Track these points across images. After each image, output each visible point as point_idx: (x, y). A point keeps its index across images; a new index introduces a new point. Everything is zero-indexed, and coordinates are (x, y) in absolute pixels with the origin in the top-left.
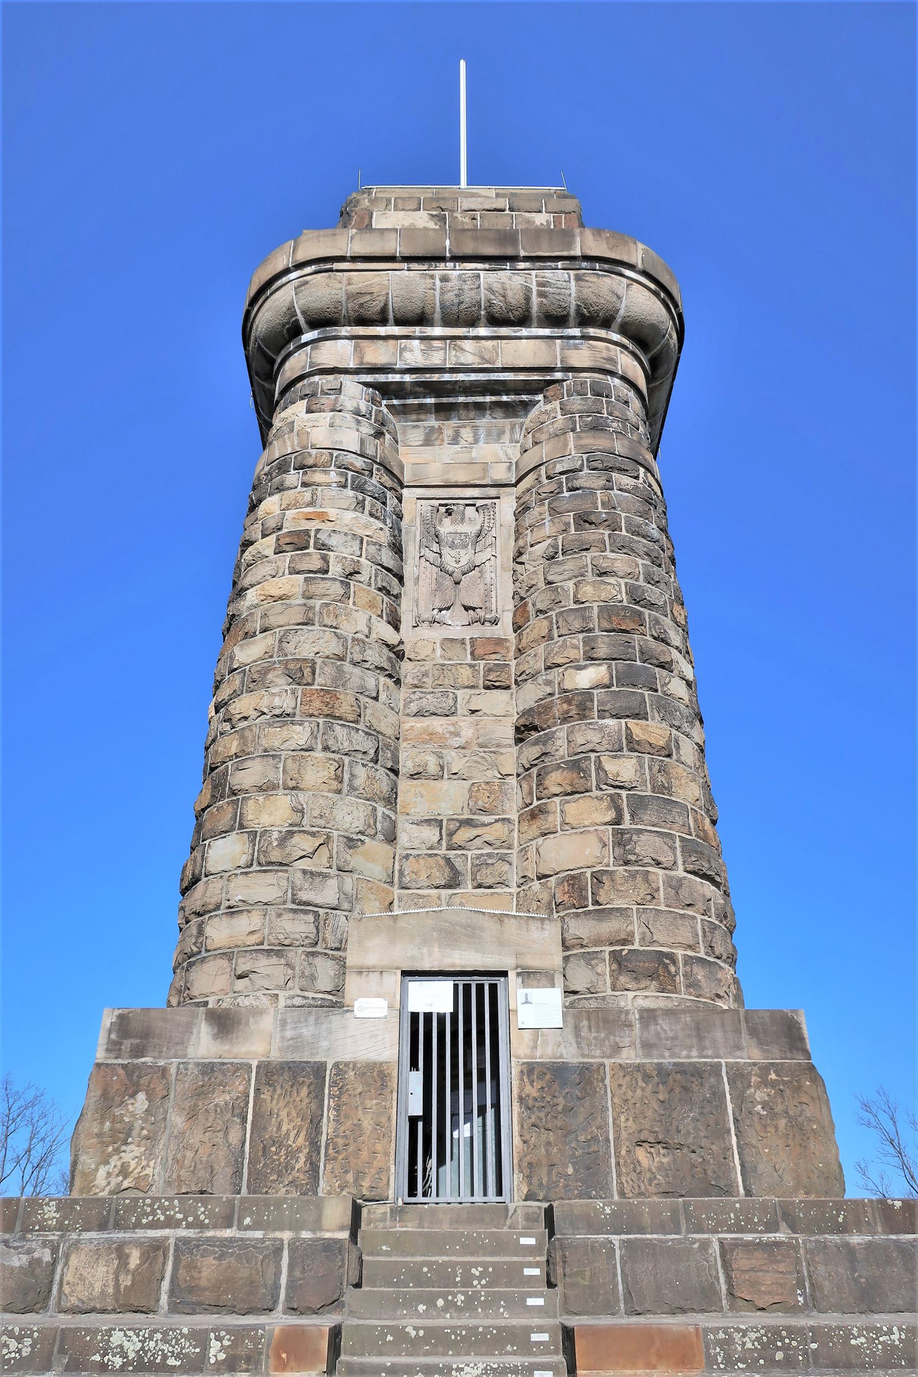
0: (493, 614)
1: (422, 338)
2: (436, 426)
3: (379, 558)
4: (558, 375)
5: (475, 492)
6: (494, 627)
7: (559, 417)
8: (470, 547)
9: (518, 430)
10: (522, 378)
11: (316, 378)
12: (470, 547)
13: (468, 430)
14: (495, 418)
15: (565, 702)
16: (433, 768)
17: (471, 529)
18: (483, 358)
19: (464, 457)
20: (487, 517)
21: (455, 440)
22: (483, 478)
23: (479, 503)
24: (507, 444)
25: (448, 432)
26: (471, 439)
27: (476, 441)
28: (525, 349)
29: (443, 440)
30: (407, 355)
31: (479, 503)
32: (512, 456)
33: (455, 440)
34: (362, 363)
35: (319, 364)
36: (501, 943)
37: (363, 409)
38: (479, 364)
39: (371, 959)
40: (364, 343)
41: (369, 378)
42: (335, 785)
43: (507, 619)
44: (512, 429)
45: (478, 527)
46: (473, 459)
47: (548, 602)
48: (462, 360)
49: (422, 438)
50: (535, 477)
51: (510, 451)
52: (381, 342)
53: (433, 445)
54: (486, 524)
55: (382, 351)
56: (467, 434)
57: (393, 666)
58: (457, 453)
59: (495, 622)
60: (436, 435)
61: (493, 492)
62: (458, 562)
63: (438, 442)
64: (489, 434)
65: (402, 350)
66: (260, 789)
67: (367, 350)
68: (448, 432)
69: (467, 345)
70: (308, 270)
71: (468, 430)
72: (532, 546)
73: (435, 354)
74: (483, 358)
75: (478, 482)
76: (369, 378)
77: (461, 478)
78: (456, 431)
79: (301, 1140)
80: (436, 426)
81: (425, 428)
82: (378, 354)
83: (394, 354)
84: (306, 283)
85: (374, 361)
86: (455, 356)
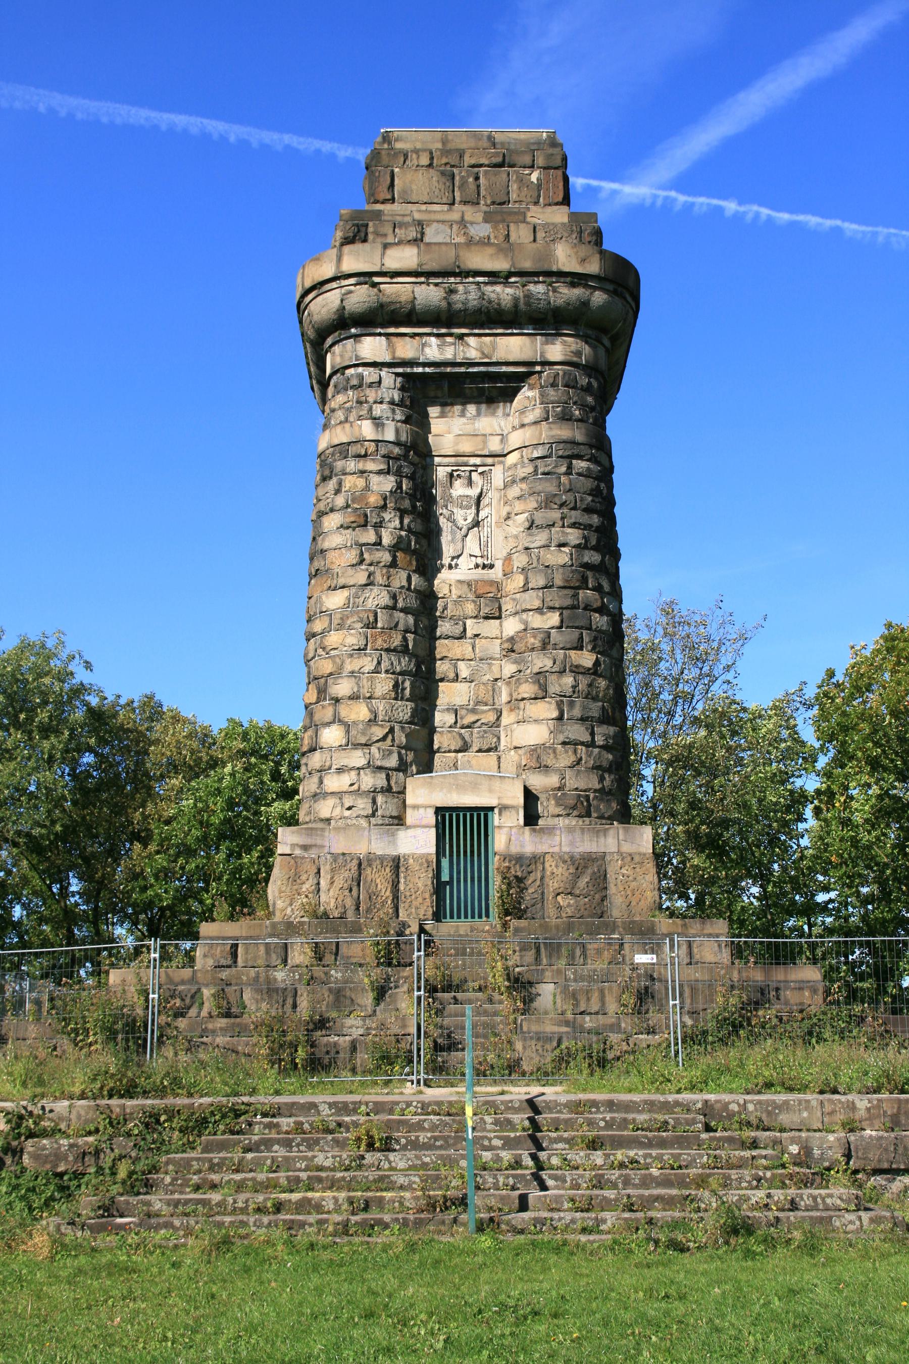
1: (438, 336)
4: (538, 368)
5: (478, 461)
6: (491, 571)
11: (360, 369)
16: (452, 675)
18: (483, 353)
19: (469, 429)
21: (463, 414)
22: (483, 449)
23: (480, 469)
28: (513, 347)
30: (427, 350)
31: (480, 469)
33: (463, 414)
34: (394, 358)
36: (490, 791)
37: (396, 398)
39: (420, 801)
40: (394, 339)
41: (400, 370)
43: (499, 565)
45: (479, 491)
48: (468, 355)
51: (502, 424)
52: (407, 338)
55: (409, 346)
61: (489, 461)
65: (424, 345)
66: (350, 698)
69: (472, 341)
70: (352, 281)
73: (447, 349)
74: (483, 353)
75: (480, 453)
76: (400, 370)
77: (466, 447)
79: (388, 893)
82: (406, 349)
83: (417, 349)
84: (351, 292)
85: (403, 356)
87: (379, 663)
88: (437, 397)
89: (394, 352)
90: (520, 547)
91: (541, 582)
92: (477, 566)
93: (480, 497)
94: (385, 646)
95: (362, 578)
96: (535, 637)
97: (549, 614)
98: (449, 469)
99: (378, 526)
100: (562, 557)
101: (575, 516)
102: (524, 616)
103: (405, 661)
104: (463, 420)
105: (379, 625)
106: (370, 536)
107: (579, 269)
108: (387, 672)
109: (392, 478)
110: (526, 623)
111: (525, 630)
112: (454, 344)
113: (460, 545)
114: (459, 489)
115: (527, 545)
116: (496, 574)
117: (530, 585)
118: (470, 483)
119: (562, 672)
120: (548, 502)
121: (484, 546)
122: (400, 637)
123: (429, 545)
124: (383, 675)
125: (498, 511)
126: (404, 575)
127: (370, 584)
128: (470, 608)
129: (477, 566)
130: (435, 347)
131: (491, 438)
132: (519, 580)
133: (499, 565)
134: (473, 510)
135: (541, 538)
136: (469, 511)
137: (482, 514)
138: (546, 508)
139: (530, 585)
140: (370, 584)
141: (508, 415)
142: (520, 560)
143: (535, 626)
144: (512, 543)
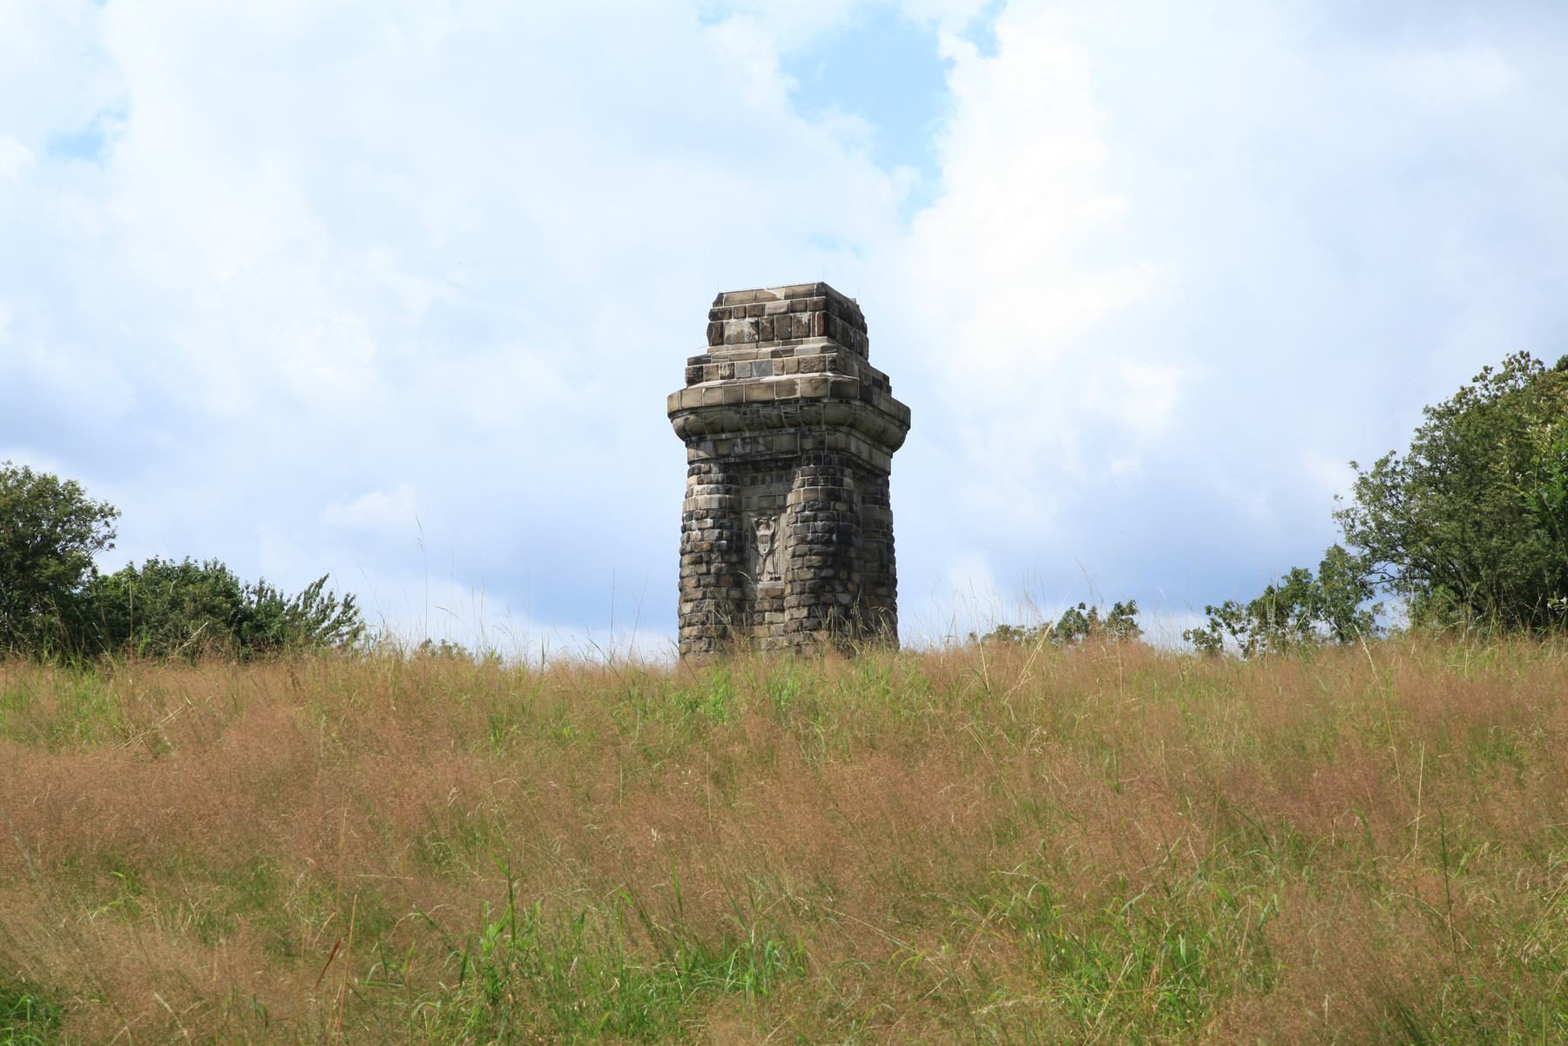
56: (768, 479)
93: (773, 535)
95: (699, 595)
99: (709, 563)
100: (809, 574)
101: (816, 547)
106: (703, 568)
107: (813, 395)
109: (717, 531)
116: (780, 584)
120: (803, 541)
121: (775, 566)
126: (724, 590)
127: (704, 597)
128: (767, 606)
135: (799, 562)
140: (704, 597)
142: (790, 577)
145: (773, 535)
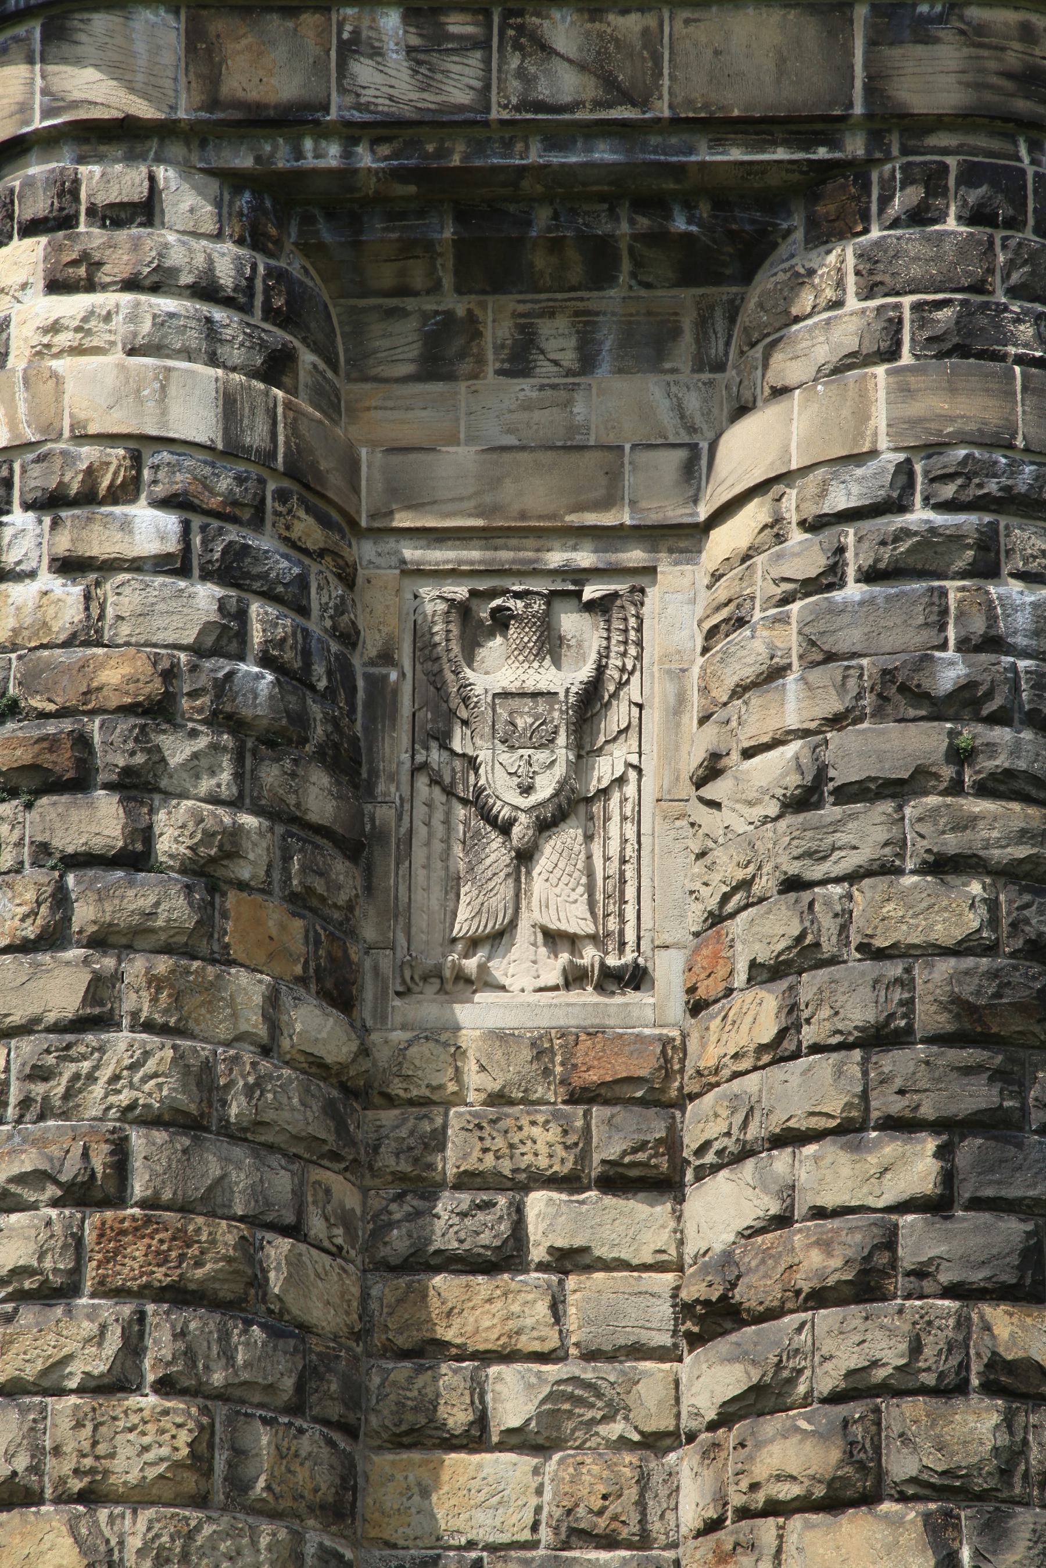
0: (629, 957)
2: (461, 311)
3: (292, 800)
6: (632, 997)
7: (852, 303)
8: (562, 740)
9: (720, 325)
10: (736, 154)
12: (562, 740)
13: (562, 323)
14: (648, 286)
15: (818, 1243)
17: (567, 678)
19: (547, 422)
20: (616, 637)
24: (686, 373)
25: (498, 329)
26: (569, 358)
27: (587, 362)
29: (481, 361)
32: (699, 421)
33: (520, 361)
34: (213, 103)
35: (75, 105)
37: (226, 274)
38: (598, 104)
42: (190, 1482)
43: (669, 972)
44: (703, 324)
45: (585, 672)
46: (573, 429)
47: (780, 946)
48: (543, 91)
49: (414, 351)
50: (765, 518)
51: (693, 402)
53: (450, 377)
54: (615, 661)
55: (279, 53)
56: (558, 341)
57: (341, 1128)
58: (527, 406)
59: (636, 978)
60: (459, 342)
61: (635, 556)
62: (527, 790)
63: (465, 367)
64: (628, 339)
67: (230, 47)
68: (498, 329)
71: (562, 323)
72: (748, 753)
73: (453, 65)
74: (609, 82)
78: (522, 328)
80: (461, 311)
81: (425, 316)
83: (319, 66)
85: (253, 95)
86: (521, 74)
87: (133, 1347)
88: (403, 291)
89: (212, 79)
90: (766, 884)
91: (859, 1012)
92: (574, 978)
93: (591, 701)
94: (160, 1275)
96: (825, 1245)
97: (891, 1148)
98: (460, 591)
102: (781, 1160)
103: (249, 1342)
104: (524, 388)
105: (138, 1188)
108: (165, 1386)
110: (789, 1191)
111: (782, 1221)
112: (483, 44)
113: (506, 890)
114: (498, 669)
115: (793, 868)
117: (809, 1035)
118: (550, 645)
119: (951, 1389)
121: (606, 895)
122: (227, 1236)
123: (369, 889)
124: (151, 1401)
125: (670, 751)
126: (249, 988)
127: (95, 1018)
129: (574, 978)
130: (396, 58)
131: (644, 457)
132: (759, 1015)
133: (669, 972)
134: (562, 752)
136: (542, 756)
137: (605, 769)
138: (879, 714)
139: (809, 1035)
140: (95, 1018)
141: (719, 367)
142: (764, 931)
143: (829, 1200)
144: (728, 868)
145: (591, 701)
